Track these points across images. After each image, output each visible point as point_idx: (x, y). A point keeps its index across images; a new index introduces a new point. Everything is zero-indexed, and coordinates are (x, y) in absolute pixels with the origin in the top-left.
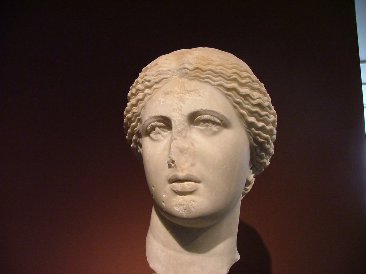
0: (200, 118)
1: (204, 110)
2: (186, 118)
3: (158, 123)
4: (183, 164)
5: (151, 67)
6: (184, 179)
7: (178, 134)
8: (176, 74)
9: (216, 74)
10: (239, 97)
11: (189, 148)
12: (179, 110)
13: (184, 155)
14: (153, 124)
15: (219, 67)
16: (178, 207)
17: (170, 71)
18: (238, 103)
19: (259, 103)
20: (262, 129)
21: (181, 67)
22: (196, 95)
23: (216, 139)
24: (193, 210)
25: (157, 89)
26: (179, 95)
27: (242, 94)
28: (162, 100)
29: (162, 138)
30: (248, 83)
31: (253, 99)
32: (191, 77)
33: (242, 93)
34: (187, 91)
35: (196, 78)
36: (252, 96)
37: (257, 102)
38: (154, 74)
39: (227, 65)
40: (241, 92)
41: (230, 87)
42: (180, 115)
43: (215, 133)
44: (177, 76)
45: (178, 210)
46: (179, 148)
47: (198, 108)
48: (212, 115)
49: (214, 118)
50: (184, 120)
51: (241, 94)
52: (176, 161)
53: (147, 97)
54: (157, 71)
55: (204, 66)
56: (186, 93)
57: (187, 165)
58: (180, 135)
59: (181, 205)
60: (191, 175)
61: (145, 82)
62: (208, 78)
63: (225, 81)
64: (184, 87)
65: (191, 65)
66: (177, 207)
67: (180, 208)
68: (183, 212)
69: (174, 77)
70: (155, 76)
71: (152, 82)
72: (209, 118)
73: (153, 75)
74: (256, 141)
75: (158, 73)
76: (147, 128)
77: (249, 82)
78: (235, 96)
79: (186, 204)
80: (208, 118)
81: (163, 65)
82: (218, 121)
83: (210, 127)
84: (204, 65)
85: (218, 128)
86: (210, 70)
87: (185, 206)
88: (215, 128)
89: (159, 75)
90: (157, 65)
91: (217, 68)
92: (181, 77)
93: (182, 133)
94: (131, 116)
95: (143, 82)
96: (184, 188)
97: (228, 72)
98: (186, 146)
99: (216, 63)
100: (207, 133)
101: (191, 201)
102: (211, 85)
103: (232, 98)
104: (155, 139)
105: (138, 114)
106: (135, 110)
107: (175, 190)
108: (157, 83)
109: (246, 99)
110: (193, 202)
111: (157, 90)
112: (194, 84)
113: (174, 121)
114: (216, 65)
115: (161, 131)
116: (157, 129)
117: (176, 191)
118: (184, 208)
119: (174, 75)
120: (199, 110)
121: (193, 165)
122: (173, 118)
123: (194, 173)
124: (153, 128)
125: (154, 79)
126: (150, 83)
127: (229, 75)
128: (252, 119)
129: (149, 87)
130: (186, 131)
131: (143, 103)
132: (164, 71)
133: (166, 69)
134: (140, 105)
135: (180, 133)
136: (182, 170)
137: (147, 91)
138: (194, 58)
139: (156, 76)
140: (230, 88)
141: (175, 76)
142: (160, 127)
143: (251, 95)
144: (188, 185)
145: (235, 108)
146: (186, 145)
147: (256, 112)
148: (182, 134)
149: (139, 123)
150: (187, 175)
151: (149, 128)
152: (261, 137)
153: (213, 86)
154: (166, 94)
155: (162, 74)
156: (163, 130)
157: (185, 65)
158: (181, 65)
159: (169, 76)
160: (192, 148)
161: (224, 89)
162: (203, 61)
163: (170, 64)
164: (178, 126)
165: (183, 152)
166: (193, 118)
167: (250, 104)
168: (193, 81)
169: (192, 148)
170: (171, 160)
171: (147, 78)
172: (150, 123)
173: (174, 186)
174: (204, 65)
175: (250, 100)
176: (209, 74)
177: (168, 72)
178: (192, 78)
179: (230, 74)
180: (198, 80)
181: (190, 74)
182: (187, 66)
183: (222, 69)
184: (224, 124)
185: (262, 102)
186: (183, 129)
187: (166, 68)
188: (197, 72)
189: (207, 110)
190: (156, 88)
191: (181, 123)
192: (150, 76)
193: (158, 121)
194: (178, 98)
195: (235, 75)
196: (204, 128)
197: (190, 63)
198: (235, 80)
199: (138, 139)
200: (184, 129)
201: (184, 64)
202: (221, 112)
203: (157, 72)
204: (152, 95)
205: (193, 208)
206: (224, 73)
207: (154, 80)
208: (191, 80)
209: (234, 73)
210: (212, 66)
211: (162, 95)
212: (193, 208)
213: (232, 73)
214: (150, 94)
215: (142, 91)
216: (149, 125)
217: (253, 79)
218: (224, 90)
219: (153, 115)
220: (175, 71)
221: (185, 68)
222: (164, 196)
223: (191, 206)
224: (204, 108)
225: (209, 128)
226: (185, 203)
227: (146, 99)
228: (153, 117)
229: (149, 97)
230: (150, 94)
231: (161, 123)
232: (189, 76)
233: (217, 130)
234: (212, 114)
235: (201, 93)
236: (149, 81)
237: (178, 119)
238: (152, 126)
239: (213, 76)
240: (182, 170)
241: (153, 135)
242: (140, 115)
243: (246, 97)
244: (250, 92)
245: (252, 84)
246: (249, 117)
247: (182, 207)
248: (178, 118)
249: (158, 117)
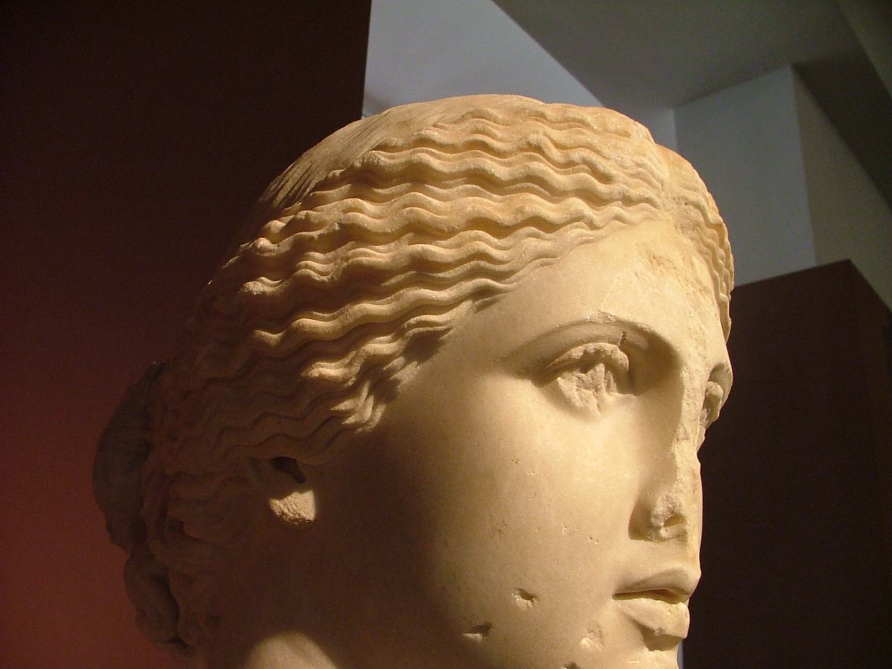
14: (608, 347)
53: (577, 227)
61: (583, 170)
76: (563, 352)
90: (627, 139)
92: (679, 226)
94: (450, 260)
104: (578, 404)
106: (486, 243)
107: (653, 625)
108: (627, 201)
111: (620, 228)
116: (601, 368)
125: (626, 184)
126: (607, 186)
131: (548, 240)
134: (532, 243)
139: (632, 176)
142: (611, 366)
149: (466, 305)
151: (577, 353)
154: (654, 258)
170: (672, 512)
171: (604, 165)
173: (651, 614)
187: (656, 168)
190: (618, 218)
199: (399, 361)
203: (638, 165)
214: (592, 225)
215: (554, 193)
216: (589, 342)
219: (626, 316)
222: (585, 642)
227: (575, 232)
228: (620, 323)
230: (592, 225)
232: (701, 239)
236: (606, 178)
241: (567, 383)
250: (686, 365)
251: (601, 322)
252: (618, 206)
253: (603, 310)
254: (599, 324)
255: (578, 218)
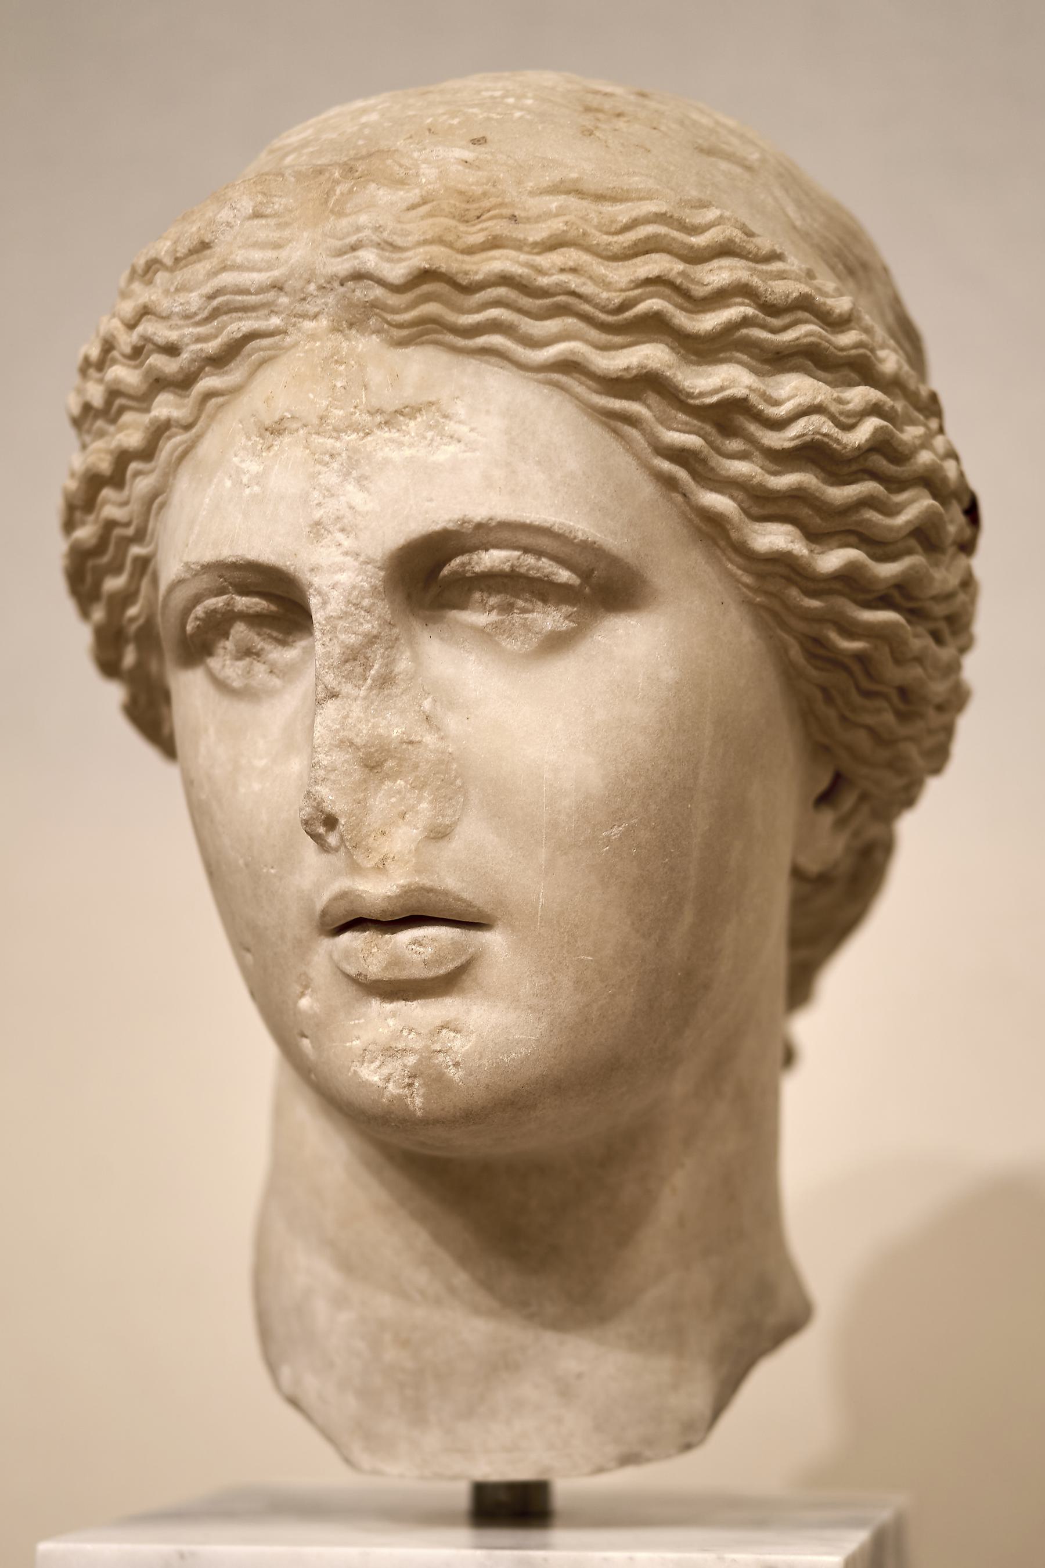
0: (463, 565)
1: (479, 526)
2: (382, 573)
3: (238, 598)
4: (383, 833)
5: (177, 260)
6: (393, 913)
7: (348, 666)
8: (313, 309)
9: (539, 302)
10: (686, 424)
11: (411, 743)
12: (343, 530)
13: (388, 784)
15: (556, 258)
16: (378, 1063)
17: (281, 289)
18: (680, 456)
19: (808, 438)
20: (848, 581)
21: (343, 266)
22: (430, 434)
23: (565, 671)
24: (455, 1074)
25: (221, 400)
26: (338, 438)
27: (697, 402)
28: (253, 467)
29: (276, 682)
30: (731, 327)
31: (778, 425)
32: (400, 326)
33: (701, 395)
34: (379, 411)
35: (427, 332)
36: (762, 406)
37: (799, 437)
38: (193, 309)
39: (608, 233)
40: (690, 395)
41: (627, 369)
42: (348, 558)
43: (556, 643)
44: (324, 322)
45: (375, 1079)
46: (358, 748)
47: (447, 518)
48: (526, 550)
49: (540, 563)
50: (374, 588)
51: (691, 401)
52: (342, 821)
54: (208, 288)
55: (467, 258)
56: (379, 426)
57: (403, 839)
58: (359, 670)
59: (390, 1052)
60: (431, 890)
62: (495, 327)
63: (594, 334)
64: (366, 387)
65: (396, 256)
66: (373, 1066)
67: (385, 1071)
68: (407, 1091)
69: (308, 325)
70: (198, 324)
71: (185, 356)
72: (512, 566)
73: (187, 317)
74: (818, 650)
75: (215, 303)
77: (746, 322)
78: (662, 422)
79: (418, 1046)
80: (507, 567)
81: (239, 256)
82: (564, 575)
83: (524, 611)
84: (470, 251)
85: (567, 617)
86: (505, 280)
87: (411, 1060)
88: (550, 619)
89: (225, 318)
90: (208, 252)
91: (545, 260)
93: (367, 658)
95: (137, 353)
96: (396, 961)
97: (607, 285)
98: (396, 733)
99: (538, 233)
100: (511, 645)
101: (443, 1027)
102: (515, 369)
103: (643, 432)
105: (130, 531)
108: (220, 361)
109: (728, 430)
110: (452, 1034)
111: (220, 407)
112: (420, 367)
113: (319, 593)
114: (535, 244)
115: (259, 643)
117: (361, 979)
118: (405, 1066)
119: (304, 316)
120: (451, 526)
121: (439, 834)
122: (317, 580)
123: (451, 878)
124: (218, 625)
125: (199, 339)
127: (617, 299)
128: (775, 538)
129: (184, 383)
130: (392, 647)
132: (246, 292)
133: (255, 276)
134: (141, 485)
135: (355, 659)
136: (381, 868)
137: (166, 407)
138: (413, 207)
140: (627, 376)
141: (315, 317)
142: (255, 620)
143: (754, 399)
144: (416, 942)
145: (669, 483)
146: (393, 725)
147: (798, 495)
148: (367, 667)
150: (407, 892)
152: (850, 630)
153: (528, 374)
155: (237, 310)
156: (270, 636)
157: (362, 253)
158: (340, 253)
159: (275, 321)
160: (430, 739)
161: (590, 383)
162: (462, 228)
163: (277, 246)
164: (341, 624)
165: (380, 764)
166: (429, 576)
167: (757, 453)
168: (410, 351)
169: (430, 739)
171: (163, 333)
172: (197, 599)
174: (470, 251)
175: (753, 428)
176: (497, 303)
177: (271, 295)
178: (405, 332)
179: (622, 290)
180: (436, 343)
181: (395, 311)
182: (369, 259)
183: (574, 270)
184: (605, 587)
185: (825, 435)
186: (372, 640)
187: (260, 270)
188: (427, 298)
189: (494, 524)
191: (356, 605)
192: (172, 322)
193: (244, 590)
194: (332, 456)
195: (651, 296)
196: (494, 617)
197: (391, 244)
198: (654, 326)
200: (376, 637)
201: (354, 248)
202: (581, 525)
203: (211, 297)
204: (194, 431)
205: (456, 1065)
206: (588, 289)
207: (199, 346)
208: (403, 343)
209: (648, 282)
210: (513, 253)
211: (249, 438)
212: (456, 1065)
213: (632, 281)
215: (144, 400)
216: (194, 606)
217: (771, 298)
218: (589, 388)
219: (209, 556)
220: (312, 287)
221: (358, 276)
222: (305, 1003)
223: (441, 1057)
224: (479, 513)
225: (517, 617)
226: (412, 1041)
227: (168, 448)
229: (184, 442)
231: (256, 600)
233: (566, 625)
234: (525, 539)
235: (460, 422)
236: (172, 350)
237: (339, 578)
238: (211, 614)
239: (520, 310)
240: (381, 868)
242: (148, 538)
243: (727, 416)
244: (750, 388)
245: (764, 327)
246: (757, 526)
247: (398, 1064)
248: (343, 578)
249: (234, 566)
250: (311, 585)
251: (188, 576)
252: (208, 375)
253: (185, 559)
254: (188, 579)
255: (160, 430)
